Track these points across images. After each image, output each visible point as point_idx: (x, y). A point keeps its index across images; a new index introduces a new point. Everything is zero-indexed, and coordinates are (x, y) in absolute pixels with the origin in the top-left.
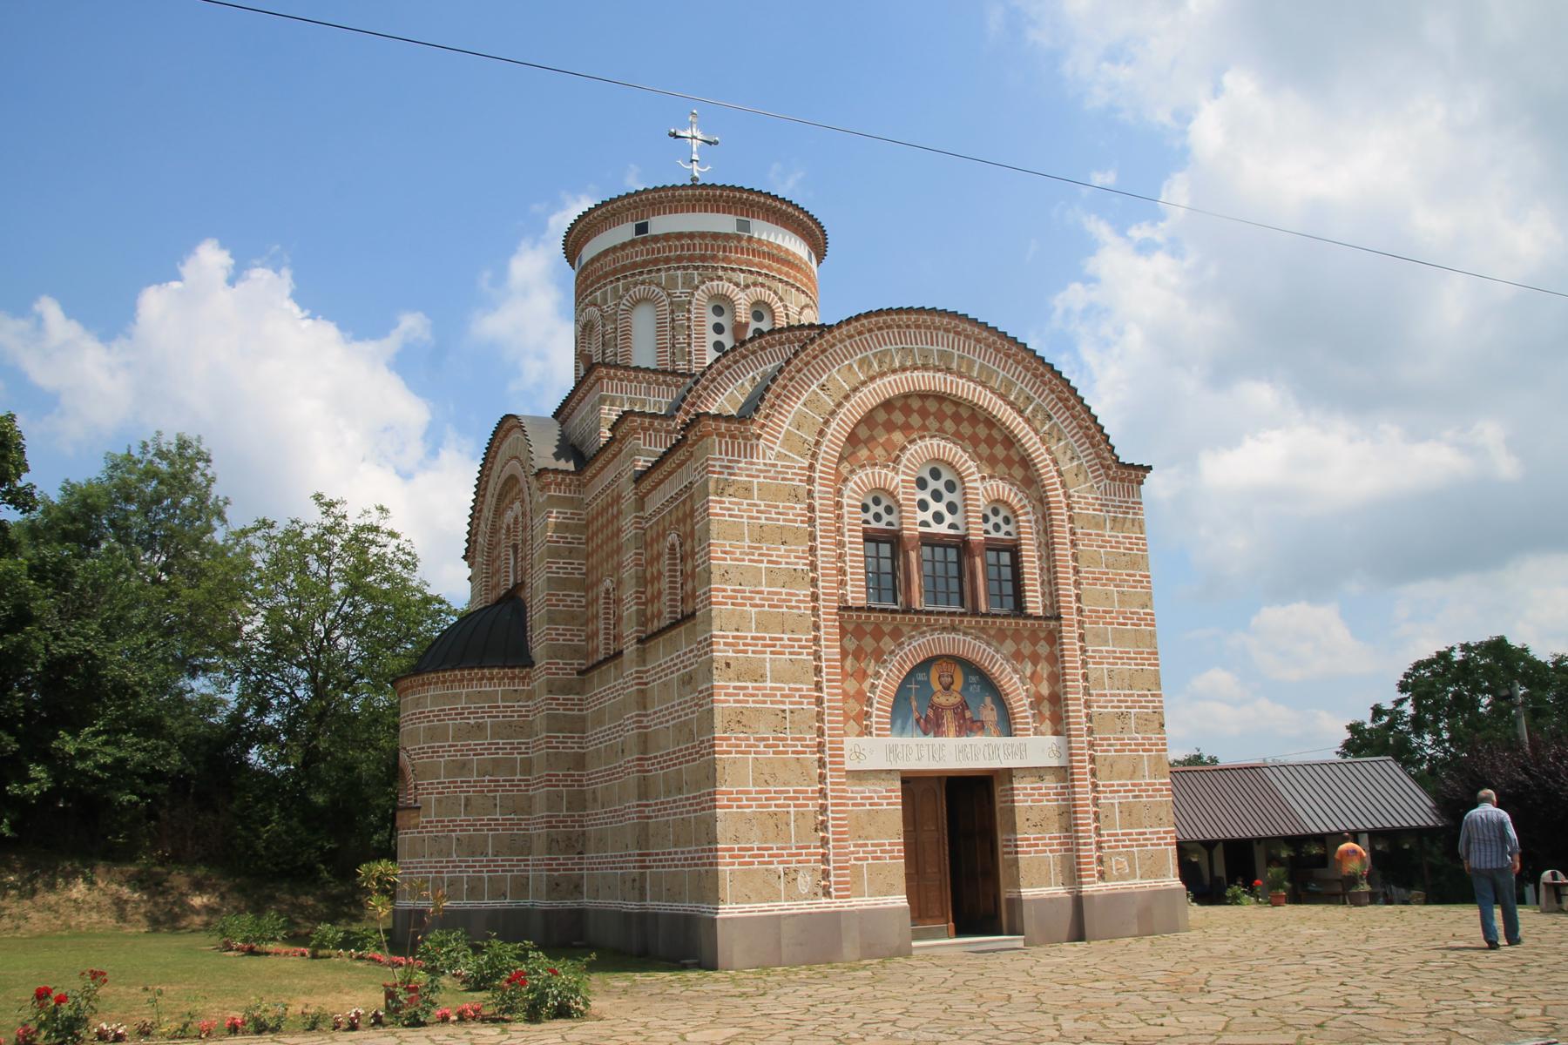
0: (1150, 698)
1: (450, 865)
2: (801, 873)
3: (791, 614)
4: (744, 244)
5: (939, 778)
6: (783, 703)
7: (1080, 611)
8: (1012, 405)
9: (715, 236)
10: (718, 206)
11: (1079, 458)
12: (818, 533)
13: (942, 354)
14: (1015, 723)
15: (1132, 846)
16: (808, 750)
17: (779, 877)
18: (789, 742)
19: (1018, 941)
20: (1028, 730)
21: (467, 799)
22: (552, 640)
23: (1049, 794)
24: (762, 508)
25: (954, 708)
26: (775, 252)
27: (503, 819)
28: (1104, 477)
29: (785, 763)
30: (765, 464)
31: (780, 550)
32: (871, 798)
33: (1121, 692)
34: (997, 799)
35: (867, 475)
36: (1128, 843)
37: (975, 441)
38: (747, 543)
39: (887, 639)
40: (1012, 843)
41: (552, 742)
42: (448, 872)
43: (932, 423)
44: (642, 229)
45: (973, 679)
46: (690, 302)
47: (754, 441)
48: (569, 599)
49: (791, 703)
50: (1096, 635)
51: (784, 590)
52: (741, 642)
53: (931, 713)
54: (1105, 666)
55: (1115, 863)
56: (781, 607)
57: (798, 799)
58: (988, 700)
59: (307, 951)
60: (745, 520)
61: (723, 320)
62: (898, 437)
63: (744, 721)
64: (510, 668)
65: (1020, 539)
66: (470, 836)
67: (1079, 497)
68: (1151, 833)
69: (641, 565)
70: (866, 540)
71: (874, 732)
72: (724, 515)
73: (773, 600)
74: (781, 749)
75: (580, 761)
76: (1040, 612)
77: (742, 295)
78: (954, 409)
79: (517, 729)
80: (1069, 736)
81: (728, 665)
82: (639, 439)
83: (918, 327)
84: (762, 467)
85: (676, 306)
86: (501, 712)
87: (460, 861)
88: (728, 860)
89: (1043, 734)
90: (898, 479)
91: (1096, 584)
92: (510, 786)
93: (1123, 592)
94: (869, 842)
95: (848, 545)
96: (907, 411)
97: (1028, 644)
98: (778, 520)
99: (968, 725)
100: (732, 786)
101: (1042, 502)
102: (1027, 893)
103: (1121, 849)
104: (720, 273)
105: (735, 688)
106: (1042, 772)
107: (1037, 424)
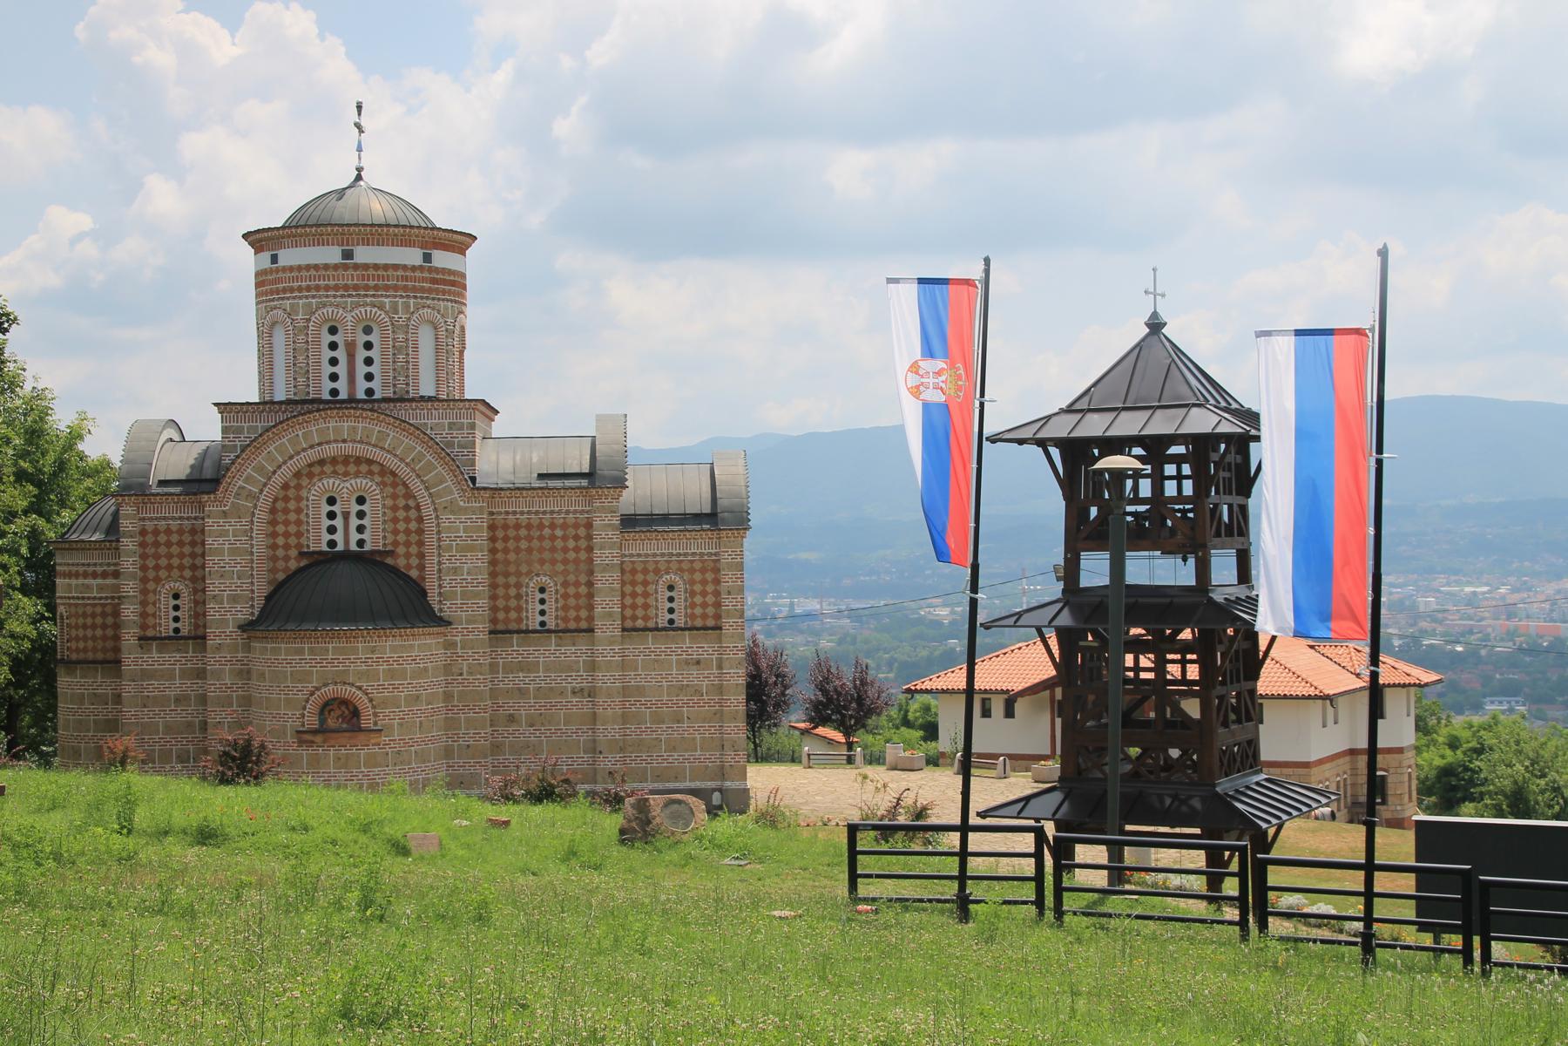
21: (421, 723)
66: (423, 749)
87: (417, 768)
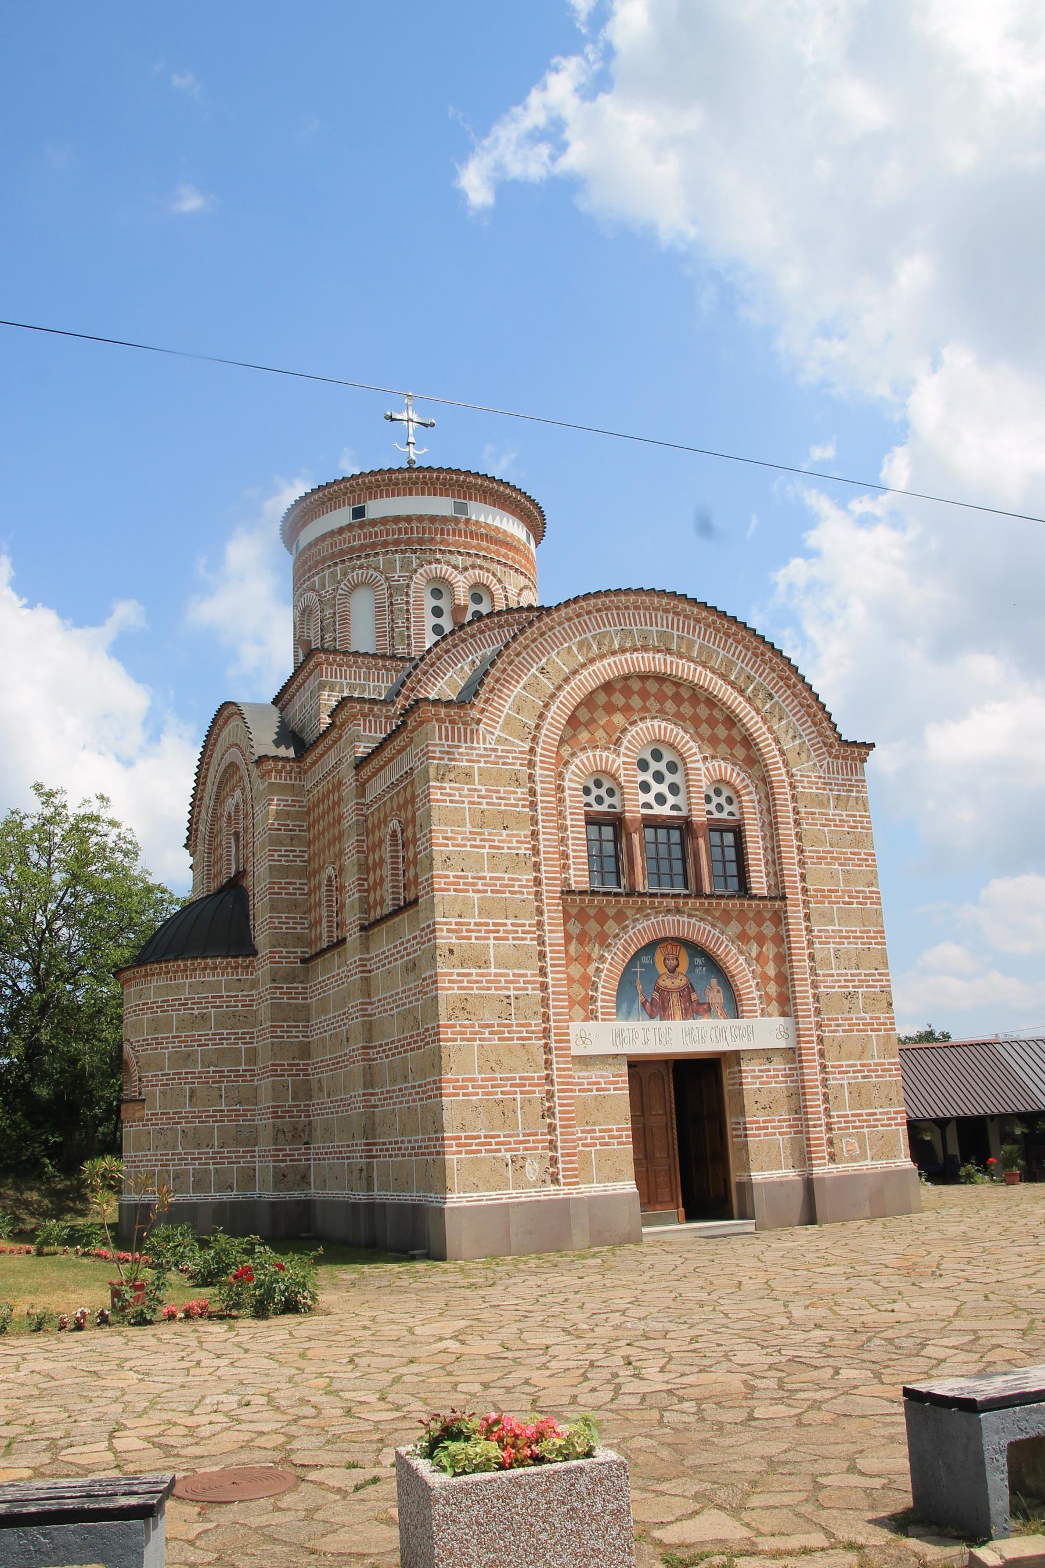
0: (878, 977)
1: (176, 1157)
2: (529, 1161)
3: (513, 899)
4: (462, 526)
5: (666, 1061)
6: (508, 989)
7: (805, 890)
8: (733, 684)
9: (433, 519)
10: (435, 489)
11: (801, 737)
12: (540, 817)
13: (661, 635)
14: (742, 1005)
15: (863, 1127)
16: (533, 1036)
17: (507, 1165)
18: (514, 1028)
19: (749, 1225)
20: (755, 1011)
21: (192, 1090)
22: (275, 928)
23: (777, 1076)
24: (484, 793)
25: (680, 991)
26: (493, 534)
27: (228, 1111)
28: (826, 755)
29: (510, 1050)
30: (485, 749)
31: (501, 835)
32: (598, 1083)
33: (849, 972)
34: (725, 1081)
35: (588, 758)
36: (858, 1124)
37: (696, 721)
38: (469, 828)
39: (611, 922)
40: (742, 1126)
41: (276, 1032)
42: (173, 1165)
43: (653, 704)
44: (359, 513)
45: (699, 961)
46: (408, 586)
47: (474, 726)
48: (291, 887)
49: (515, 989)
50: (823, 915)
51: (506, 876)
52: (464, 928)
53: (656, 996)
54: (832, 946)
55: (846, 1144)
56: (504, 892)
57: (524, 1085)
58: (714, 982)
59: (33, 1248)
60: (466, 805)
61: (443, 603)
62: (618, 719)
63: (469, 1007)
64: (233, 957)
65: (744, 819)
66: (195, 1128)
67: (802, 776)
68: (881, 1113)
69: (363, 852)
70: (588, 823)
71: (600, 1016)
72: (445, 801)
73: (496, 885)
74: (506, 1035)
75: (305, 1051)
76: (765, 892)
77: (460, 577)
78: (675, 689)
79: (241, 1018)
80: (797, 1017)
81: (451, 951)
82: (359, 725)
83: (637, 608)
84: (482, 752)
85: (393, 590)
86: (225, 1002)
87: (186, 1154)
88: (455, 1149)
89: (770, 1015)
90: (619, 762)
91: (820, 864)
92: (235, 1076)
93: (848, 871)
94: (597, 1128)
95: (570, 829)
96: (627, 692)
97: (753, 925)
98: (500, 805)
99: (694, 1008)
100: (457, 1073)
101: (765, 781)
102: (757, 1176)
103: (852, 1131)
104: (438, 556)
105: (458, 974)
106: (770, 1054)
107: (758, 703)
